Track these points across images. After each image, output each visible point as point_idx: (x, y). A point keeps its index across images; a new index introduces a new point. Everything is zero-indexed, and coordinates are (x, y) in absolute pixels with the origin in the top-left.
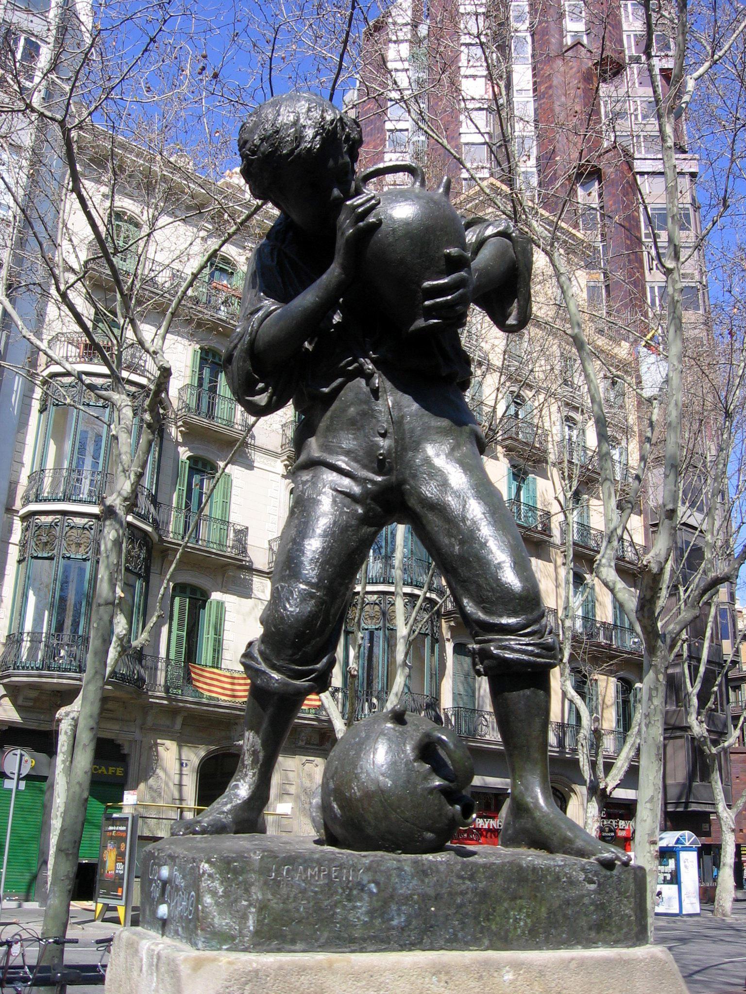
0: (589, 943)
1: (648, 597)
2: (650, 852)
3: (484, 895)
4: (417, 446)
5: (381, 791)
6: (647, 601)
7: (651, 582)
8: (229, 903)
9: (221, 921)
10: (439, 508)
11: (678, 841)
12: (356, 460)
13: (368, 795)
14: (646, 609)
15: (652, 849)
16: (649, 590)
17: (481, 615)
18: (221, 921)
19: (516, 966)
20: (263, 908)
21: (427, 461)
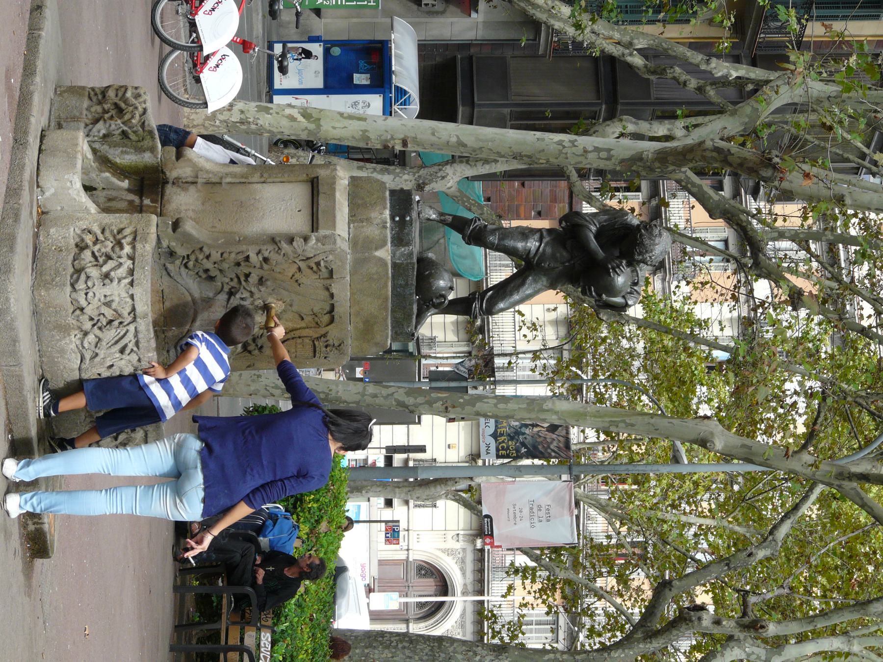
0: (392, 330)
1: (730, 158)
2: (392, 138)
3: (405, 308)
4: (545, 275)
5: (431, 287)
6: (726, 157)
7: (751, 165)
8: (403, 255)
9: (398, 253)
10: (523, 284)
11: (401, 92)
12: (541, 256)
13: (430, 283)
14: (714, 154)
15: (397, 141)
16: (739, 161)
17: (487, 297)
18: (398, 253)
19: (387, 315)
20: (402, 264)
21: (540, 278)
